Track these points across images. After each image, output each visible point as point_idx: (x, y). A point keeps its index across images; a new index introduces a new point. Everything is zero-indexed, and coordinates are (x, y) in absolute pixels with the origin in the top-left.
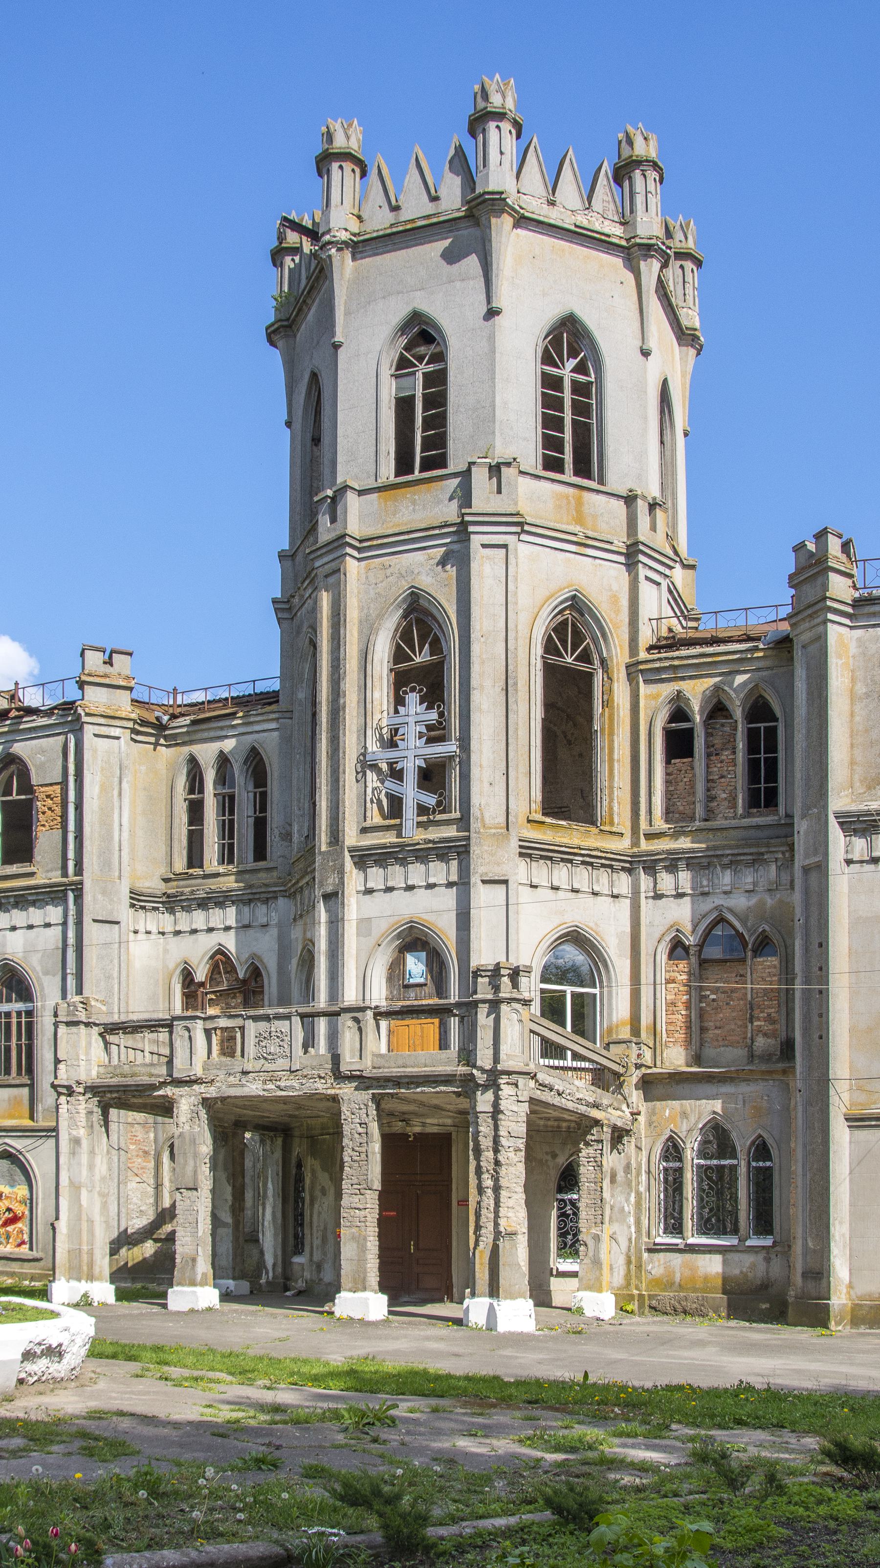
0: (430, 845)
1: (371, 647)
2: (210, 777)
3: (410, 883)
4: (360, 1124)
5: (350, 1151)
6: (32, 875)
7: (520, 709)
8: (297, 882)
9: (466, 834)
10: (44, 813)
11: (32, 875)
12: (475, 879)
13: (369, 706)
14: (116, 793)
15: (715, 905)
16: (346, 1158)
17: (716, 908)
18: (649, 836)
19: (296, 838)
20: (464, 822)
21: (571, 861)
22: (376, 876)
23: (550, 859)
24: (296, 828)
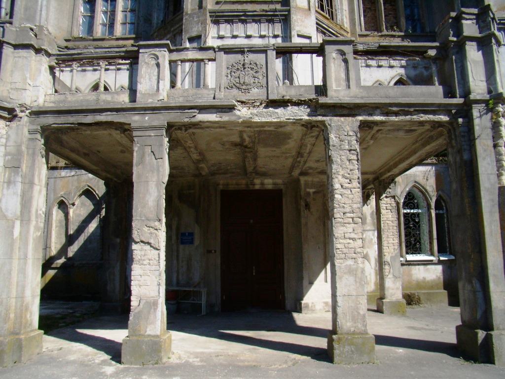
0: (264, 13)
3: (249, 33)
4: (350, 150)
5: (340, 177)
9: (289, 8)
15: (398, 73)
16: (337, 186)
17: (399, 74)
18: (360, 36)
19: (155, 21)
24: (155, 15)
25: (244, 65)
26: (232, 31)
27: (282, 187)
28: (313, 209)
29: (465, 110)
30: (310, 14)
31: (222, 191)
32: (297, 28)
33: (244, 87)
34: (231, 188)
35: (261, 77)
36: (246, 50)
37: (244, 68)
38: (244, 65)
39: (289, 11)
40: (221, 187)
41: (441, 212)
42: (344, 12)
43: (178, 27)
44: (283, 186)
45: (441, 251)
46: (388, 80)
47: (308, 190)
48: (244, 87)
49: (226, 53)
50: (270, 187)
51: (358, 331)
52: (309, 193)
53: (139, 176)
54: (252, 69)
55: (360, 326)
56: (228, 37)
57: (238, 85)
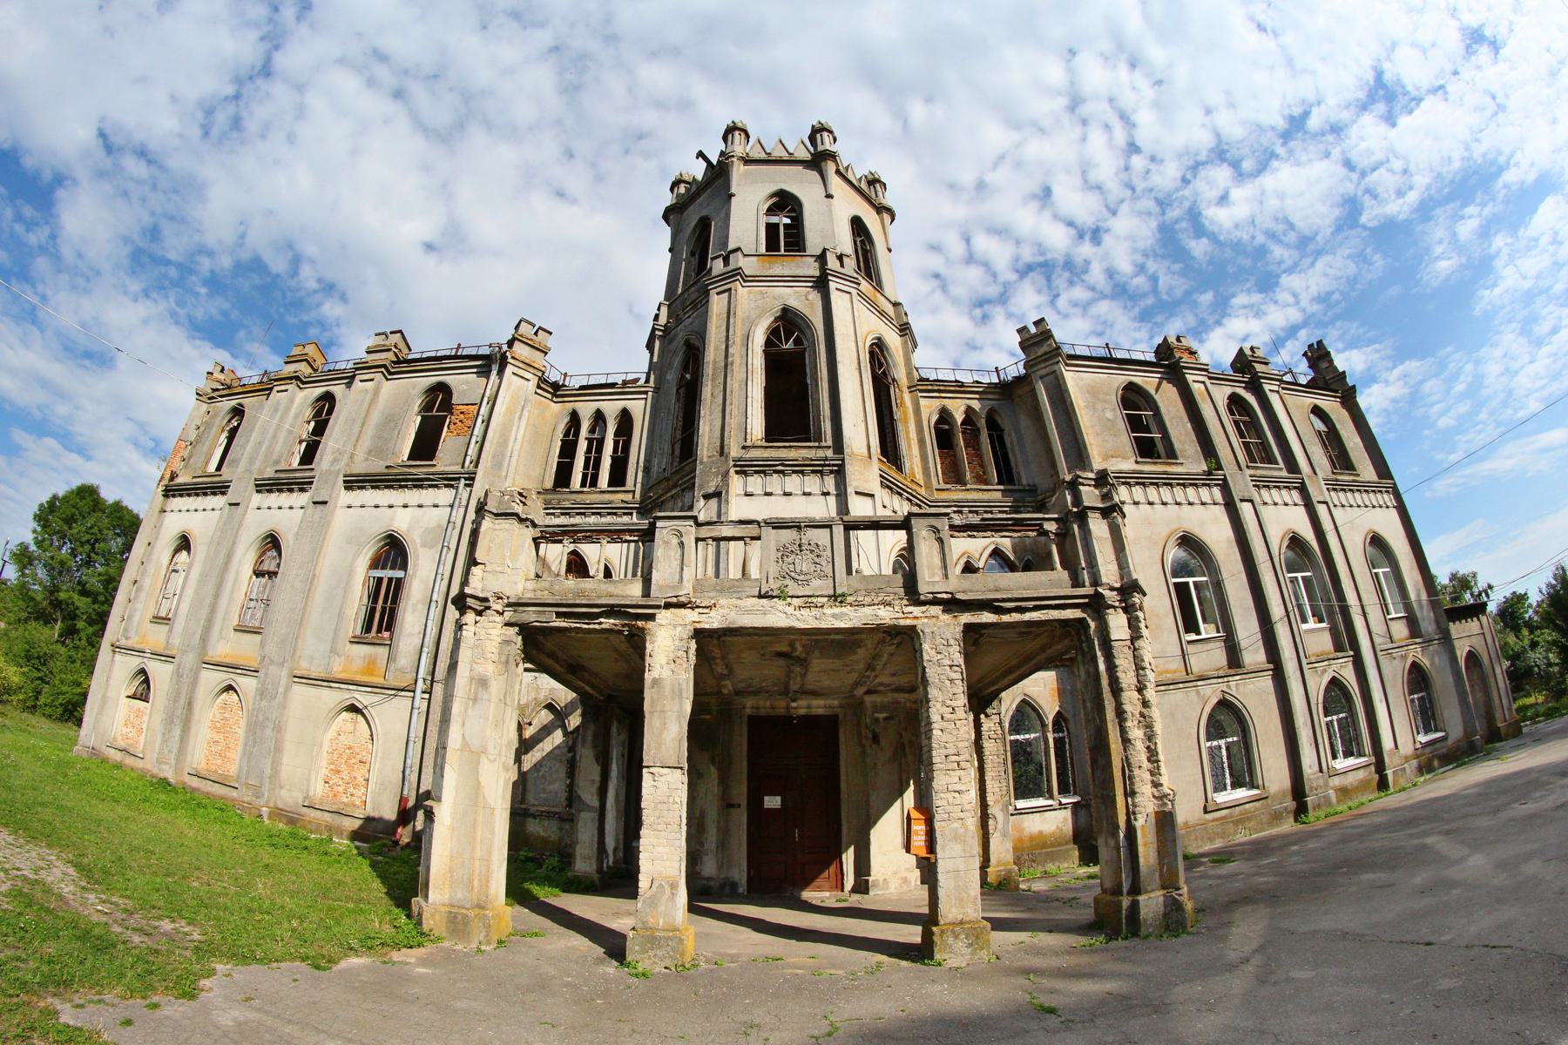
1: (751, 334)
2: (585, 426)
4: (951, 666)
5: (939, 705)
6: (435, 465)
7: (865, 386)
8: (660, 497)
10: (455, 424)
11: (435, 465)
12: (850, 490)
13: (750, 367)
14: (517, 416)
16: (935, 717)
20: (838, 445)
21: (901, 495)
22: (755, 483)
23: (891, 489)
25: (800, 546)
26: (764, 486)
27: (839, 711)
28: (884, 742)
29: (1096, 605)
30: (871, 464)
31: (749, 717)
32: (855, 483)
33: (802, 577)
34: (763, 712)
35: (824, 564)
36: (803, 524)
37: (801, 551)
38: (800, 546)
39: (843, 460)
40: (748, 711)
41: (1061, 735)
42: (915, 459)
43: (687, 481)
44: (839, 710)
45: (1064, 790)
46: (980, 551)
47: (876, 715)
48: (802, 577)
49: (774, 528)
50: (821, 711)
51: (968, 919)
52: (877, 720)
53: (653, 702)
54: (812, 551)
55: (970, 911)
56: (759, 495)
57: (793, 574)
